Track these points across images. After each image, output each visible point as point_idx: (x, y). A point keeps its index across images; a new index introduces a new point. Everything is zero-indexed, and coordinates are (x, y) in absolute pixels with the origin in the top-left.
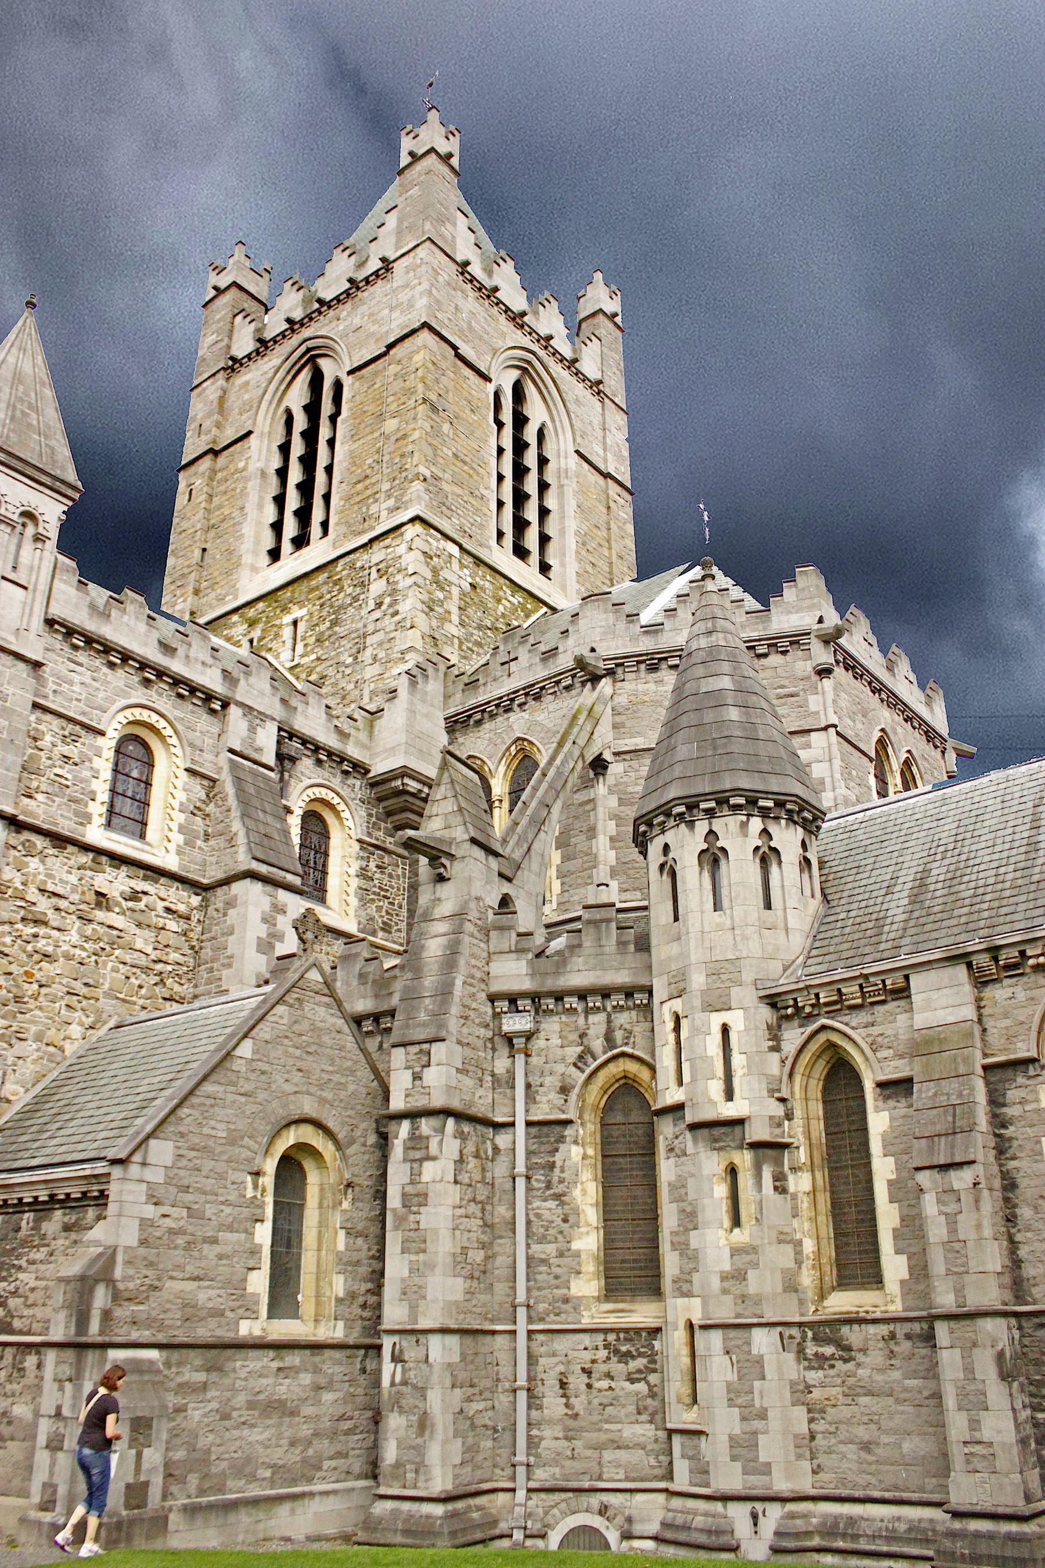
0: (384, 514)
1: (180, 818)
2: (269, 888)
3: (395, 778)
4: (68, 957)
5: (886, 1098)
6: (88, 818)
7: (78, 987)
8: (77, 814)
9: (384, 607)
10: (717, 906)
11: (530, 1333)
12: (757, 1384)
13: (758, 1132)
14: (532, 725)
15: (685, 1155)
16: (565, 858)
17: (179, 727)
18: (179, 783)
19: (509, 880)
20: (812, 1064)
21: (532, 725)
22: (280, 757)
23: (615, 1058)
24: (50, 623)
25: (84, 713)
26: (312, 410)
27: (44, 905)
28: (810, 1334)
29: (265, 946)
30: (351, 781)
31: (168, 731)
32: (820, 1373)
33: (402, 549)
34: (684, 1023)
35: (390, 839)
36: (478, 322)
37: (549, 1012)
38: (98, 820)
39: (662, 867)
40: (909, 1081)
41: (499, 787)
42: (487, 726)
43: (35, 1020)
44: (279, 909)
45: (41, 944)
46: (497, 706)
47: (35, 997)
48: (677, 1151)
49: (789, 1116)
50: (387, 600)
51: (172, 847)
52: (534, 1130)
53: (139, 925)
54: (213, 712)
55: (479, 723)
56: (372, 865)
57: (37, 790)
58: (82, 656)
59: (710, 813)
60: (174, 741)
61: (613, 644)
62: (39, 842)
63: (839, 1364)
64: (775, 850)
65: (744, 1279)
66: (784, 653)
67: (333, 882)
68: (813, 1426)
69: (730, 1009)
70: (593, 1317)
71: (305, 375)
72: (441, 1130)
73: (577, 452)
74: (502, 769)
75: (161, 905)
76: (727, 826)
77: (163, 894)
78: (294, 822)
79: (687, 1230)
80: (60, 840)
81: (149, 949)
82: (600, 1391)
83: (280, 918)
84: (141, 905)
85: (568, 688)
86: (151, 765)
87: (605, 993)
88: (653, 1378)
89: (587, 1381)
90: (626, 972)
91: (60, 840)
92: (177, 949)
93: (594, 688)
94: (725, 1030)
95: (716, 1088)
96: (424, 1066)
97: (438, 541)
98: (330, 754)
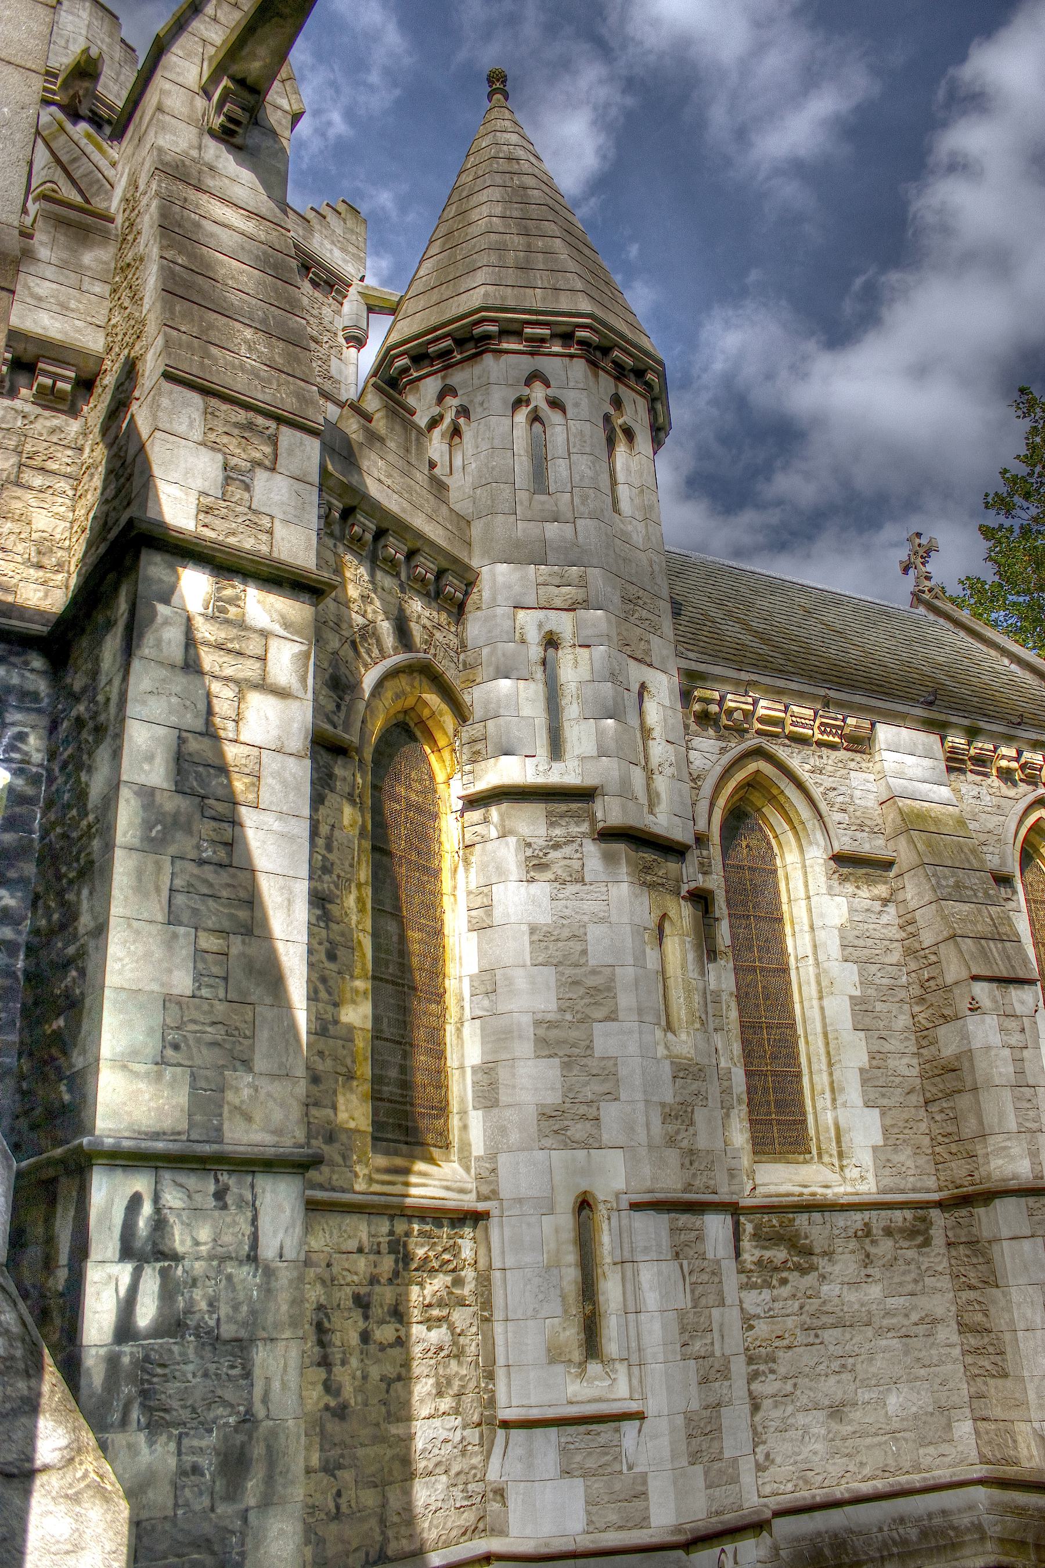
5: (844, 879)
12: (716, 1313)
15: (582, 881)
28: (749, 1228)
32: (766, 1294)
48: (558, 869)
63: (793, 1277)
65: (692, 1123)
68: (755, 1386)
69: (650, 665)
70: (371, 1180)
79: (585, 1020)
82: (382, 1348)
88: (460, 1317)
89: (361, 1324)
90: (440, 531)
96: (257, 464)
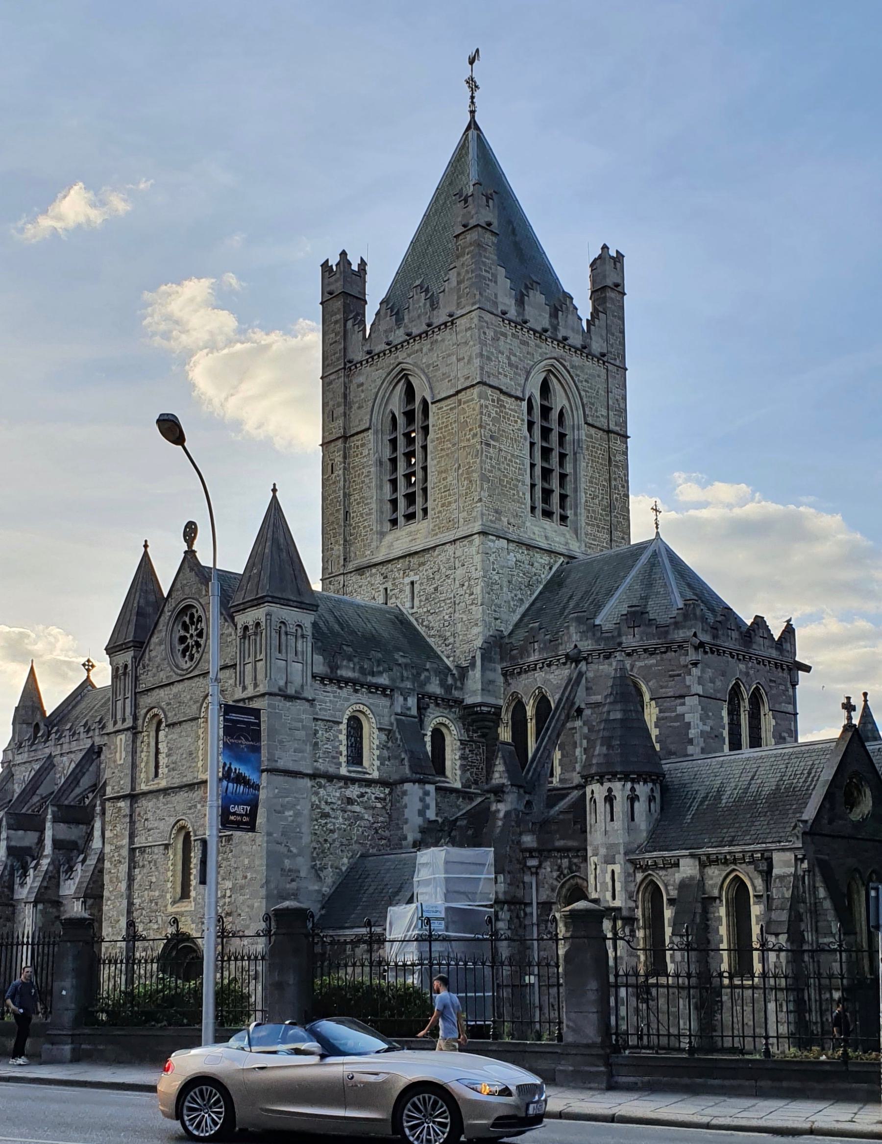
0: (461, 520)
1: (377, 752)
2: (421, 785)
3: (477, 706)
4: (339, 829)
6: (340, 764)
7: (344, 841)
8: (336, 764)
9: (465, 588)
10: (612, 820)
11: (540, 987)
13: (625, 913)
14: (546, 681)
16: (563, 755)
17: (372, 707)
18: (375, 736)
19: (530, 793)
20: (646, 888)
21: (546, 681)
22: (419, 708)
23: (573, 877)
24: (314, 677)
25: (332, 716)
26: (410, 416)
27: (327, 809)
29: (422, 813)
30: (453, 710)
31: (369, 712)
33: (474, 549)
34: (598, 867)
35: (475, 735)
36: (515, 355)
37: (547, 858)
38: (344, 765)
39: (591, 799)
40: (675, 899)
41: (530, 711)
42: (524, 676)
43: (328, 861)
44: (427, 793)
45: (329, 826)
46: (528, 666)
47: (329, 849)
49: (637, 907)
50: (466, 584)
51: (375, 768)
52: (540, 906)
53: (365, 808)
54: (386, 695)
55: (519, 674)
56: (467, 750)
57: (319, 758)
58: (328, 688)
59: (609, 780)
60: (371, 716)
61: (586, 643)
62: (323, 781)
64: (637, 797)
66: (675, 651)
67: (448, 764)
71: (401, 387)
72: (502, 909)
73: (586, 423)
74: (531, 702)
75: (373, 796)
76: (617, 786)
77: (374, 791)
78: (428, 739)
80: (331, 778)
81: (370, 819)
83: (427, 798)
84: (365, 798)
85: (565, 664)
86: (361, 727)
87: (568, 849)
91: (331, 778)
92: (382, 816)
93: (577, 666)
94: (613, 872)
95: (609, 895)
97: (494, 541)
98: (443, 700)
